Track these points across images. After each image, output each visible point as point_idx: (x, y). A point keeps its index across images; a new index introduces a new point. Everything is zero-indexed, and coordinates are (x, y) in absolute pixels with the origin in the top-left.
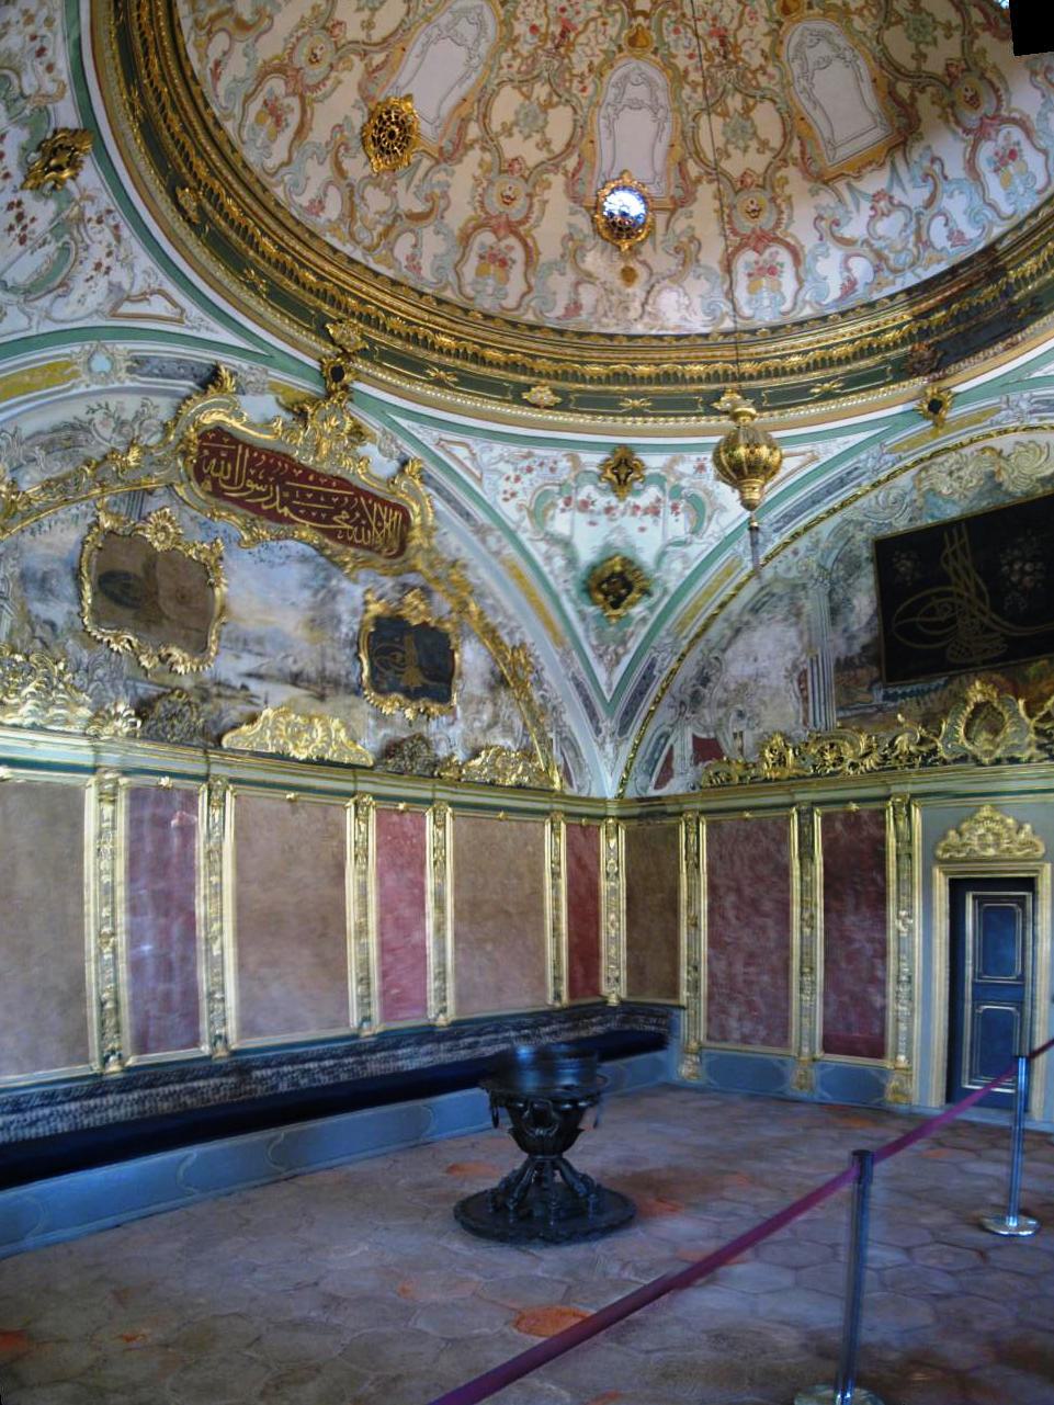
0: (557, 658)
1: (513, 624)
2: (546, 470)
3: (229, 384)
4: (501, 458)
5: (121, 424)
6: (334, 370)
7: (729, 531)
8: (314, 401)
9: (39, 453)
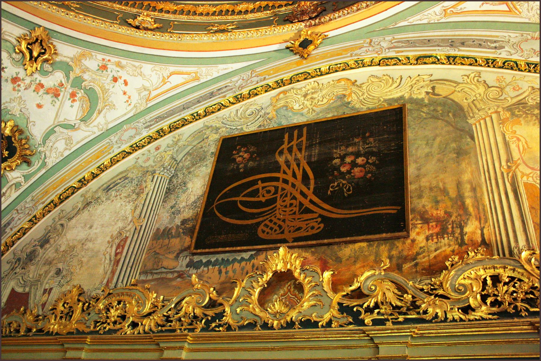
7: (111, 126)
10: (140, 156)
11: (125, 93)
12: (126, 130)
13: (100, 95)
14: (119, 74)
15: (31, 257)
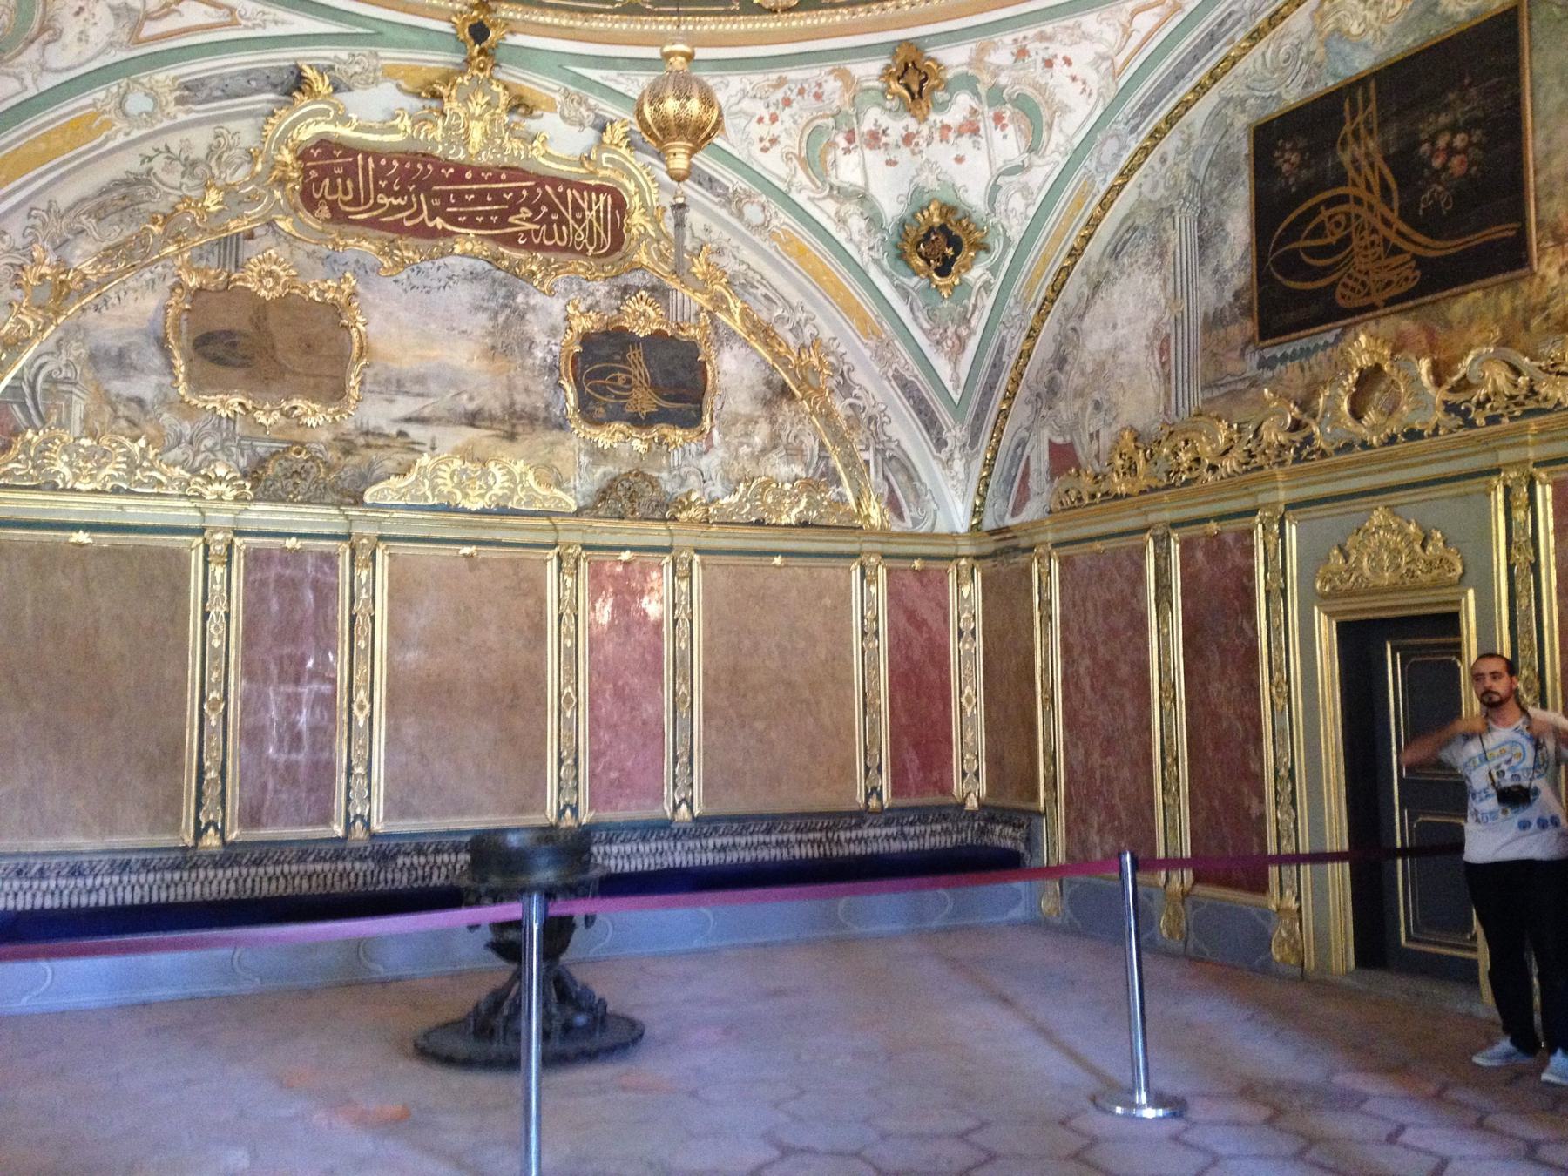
0: (868, 353)
1: (801, 316)
2: (809, 99)
3: (322, 86)
4: (744, 94)
5: (191, 165)
6: (471, 28)
7: (1077, 141)
8: (447, 79)
9: (89, 223)
10: (1142, 180)
11: (1074, 79)
12: (1103, 143)
13: (1038, 99)
14: (1051, 52)
15: (1053, 388)
